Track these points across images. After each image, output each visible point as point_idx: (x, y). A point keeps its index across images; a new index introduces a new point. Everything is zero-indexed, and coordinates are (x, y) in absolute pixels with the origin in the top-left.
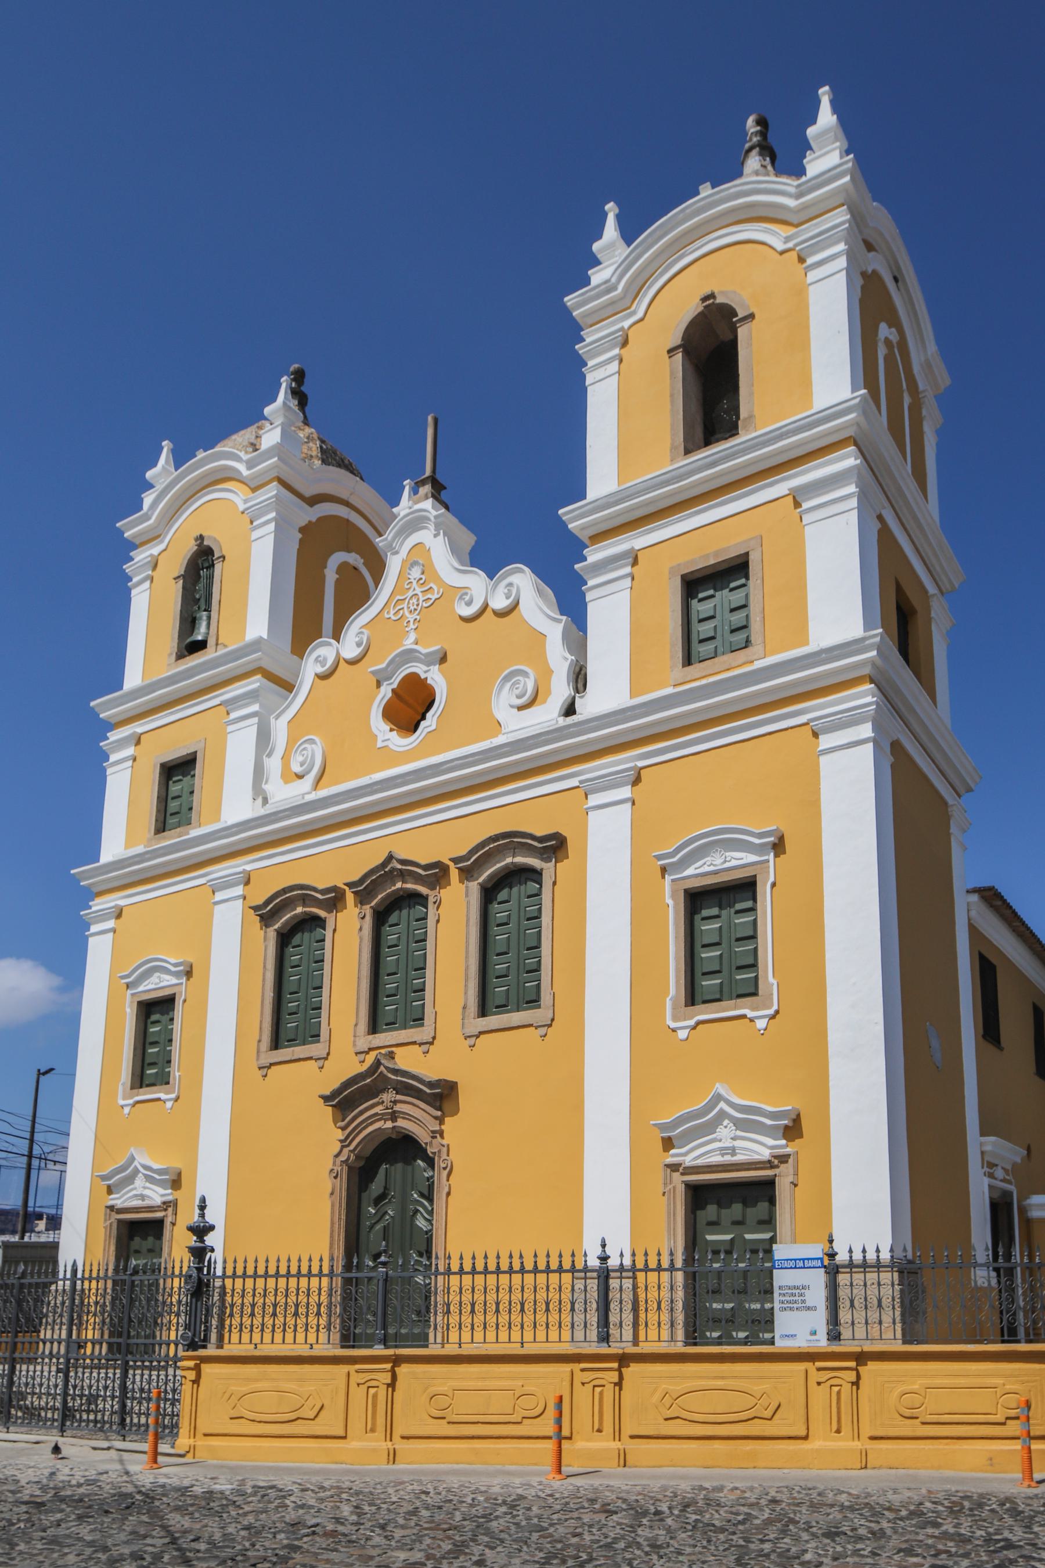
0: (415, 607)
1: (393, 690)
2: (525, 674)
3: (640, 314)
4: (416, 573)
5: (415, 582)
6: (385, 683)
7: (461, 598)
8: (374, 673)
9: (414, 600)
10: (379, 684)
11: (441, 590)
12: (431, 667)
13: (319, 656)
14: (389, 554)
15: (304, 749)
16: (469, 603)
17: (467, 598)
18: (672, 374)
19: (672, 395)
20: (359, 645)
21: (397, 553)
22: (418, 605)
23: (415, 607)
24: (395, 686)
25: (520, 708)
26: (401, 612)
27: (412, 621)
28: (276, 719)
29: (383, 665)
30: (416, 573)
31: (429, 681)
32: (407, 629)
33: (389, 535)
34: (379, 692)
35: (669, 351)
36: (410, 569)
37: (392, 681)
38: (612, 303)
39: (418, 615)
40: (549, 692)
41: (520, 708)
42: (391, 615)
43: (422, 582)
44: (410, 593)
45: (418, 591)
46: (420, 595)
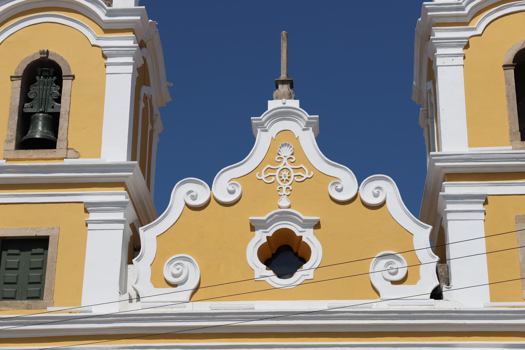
0: (287, 178)
1: (268, 237)
2: (399, 259)
3: (479, 32)
4: (286, 152)
5: (285, 160)
6: (261, 231)
7: (333, 184)
8: (251, 220)
9: (285, 173)
10: (253, 229)
11: (312, 173)
12: (307, 230)
13: (191, 191)
14: (259, 130)
15: (178, 264)
16: (340, 190)
17: (339, 187)
18: (507, 82)
19: (508, 96)
20: (232, 192)
21: (266, 131)
22: (289, 177)
23: (287, 178)
24: (270, 234)
25: (394, 283)
26: (273, 178)
27: (284, 188)
28: (144, 231)
29: (265, 218)
30: (286, 152)
31: (304, 239)
32: (280, 193)
33: (264, 117)
34: (254, 235)
35: (504, 66)
36: (280, 148)
37: (268, 230)
38: (458, 16)
39: (290, 185)
40: (417, 278)
41: (394, 283)
42: (263, 177)
43: (292, 161)
44: (281, 166)
45: (289, 166)
46: (291, 170)
